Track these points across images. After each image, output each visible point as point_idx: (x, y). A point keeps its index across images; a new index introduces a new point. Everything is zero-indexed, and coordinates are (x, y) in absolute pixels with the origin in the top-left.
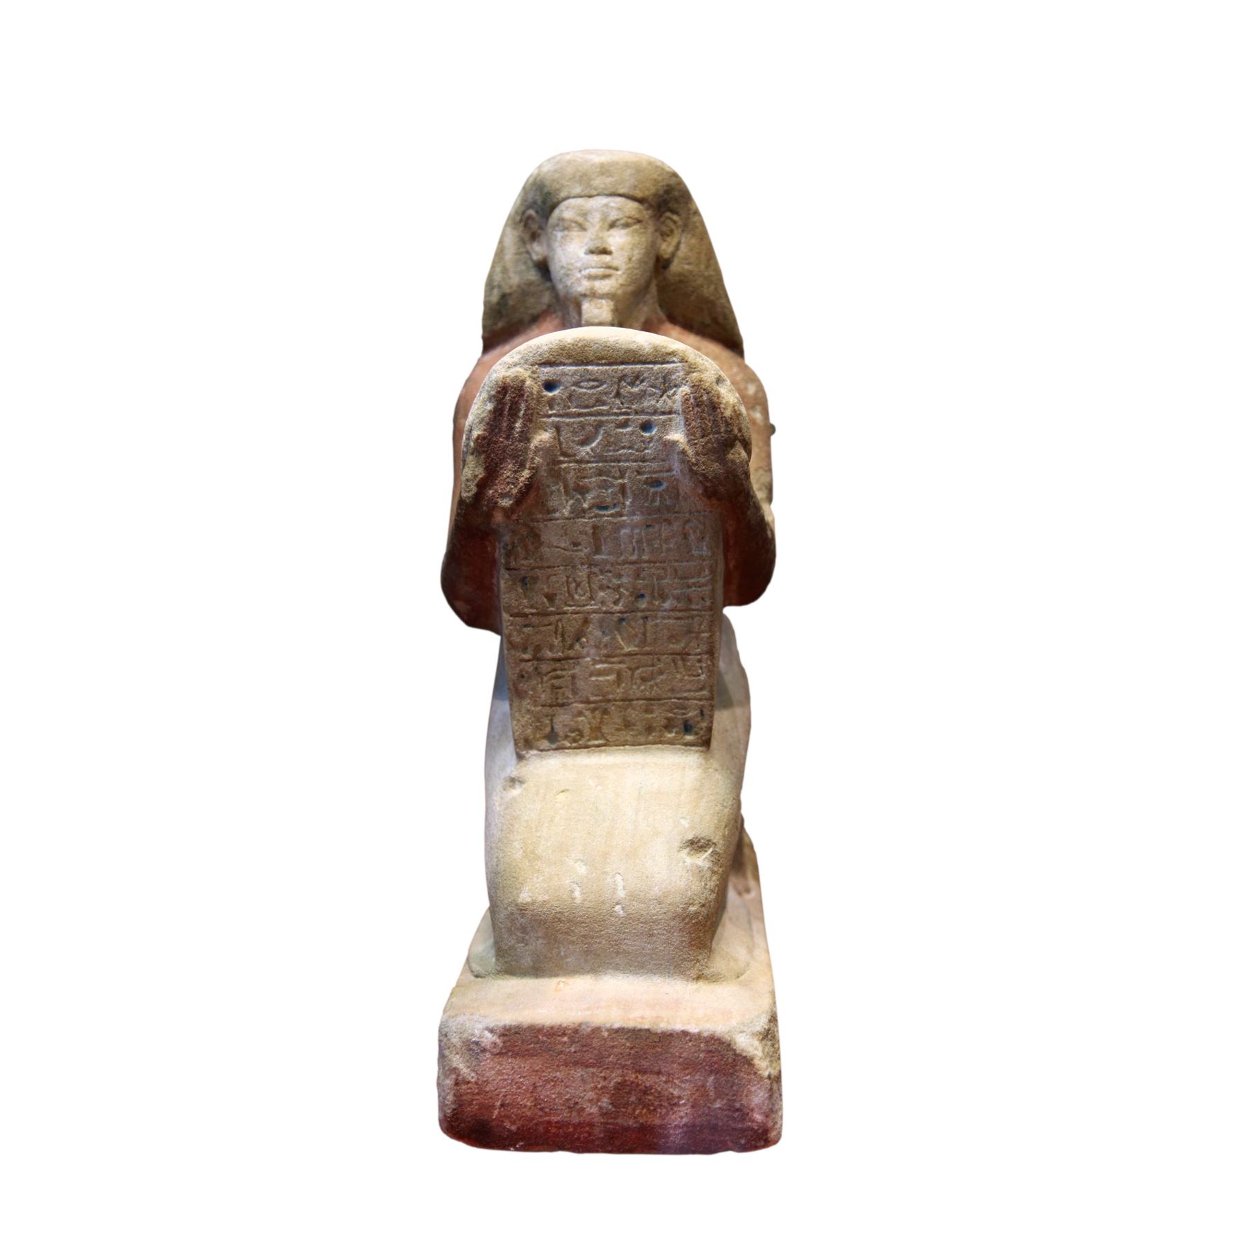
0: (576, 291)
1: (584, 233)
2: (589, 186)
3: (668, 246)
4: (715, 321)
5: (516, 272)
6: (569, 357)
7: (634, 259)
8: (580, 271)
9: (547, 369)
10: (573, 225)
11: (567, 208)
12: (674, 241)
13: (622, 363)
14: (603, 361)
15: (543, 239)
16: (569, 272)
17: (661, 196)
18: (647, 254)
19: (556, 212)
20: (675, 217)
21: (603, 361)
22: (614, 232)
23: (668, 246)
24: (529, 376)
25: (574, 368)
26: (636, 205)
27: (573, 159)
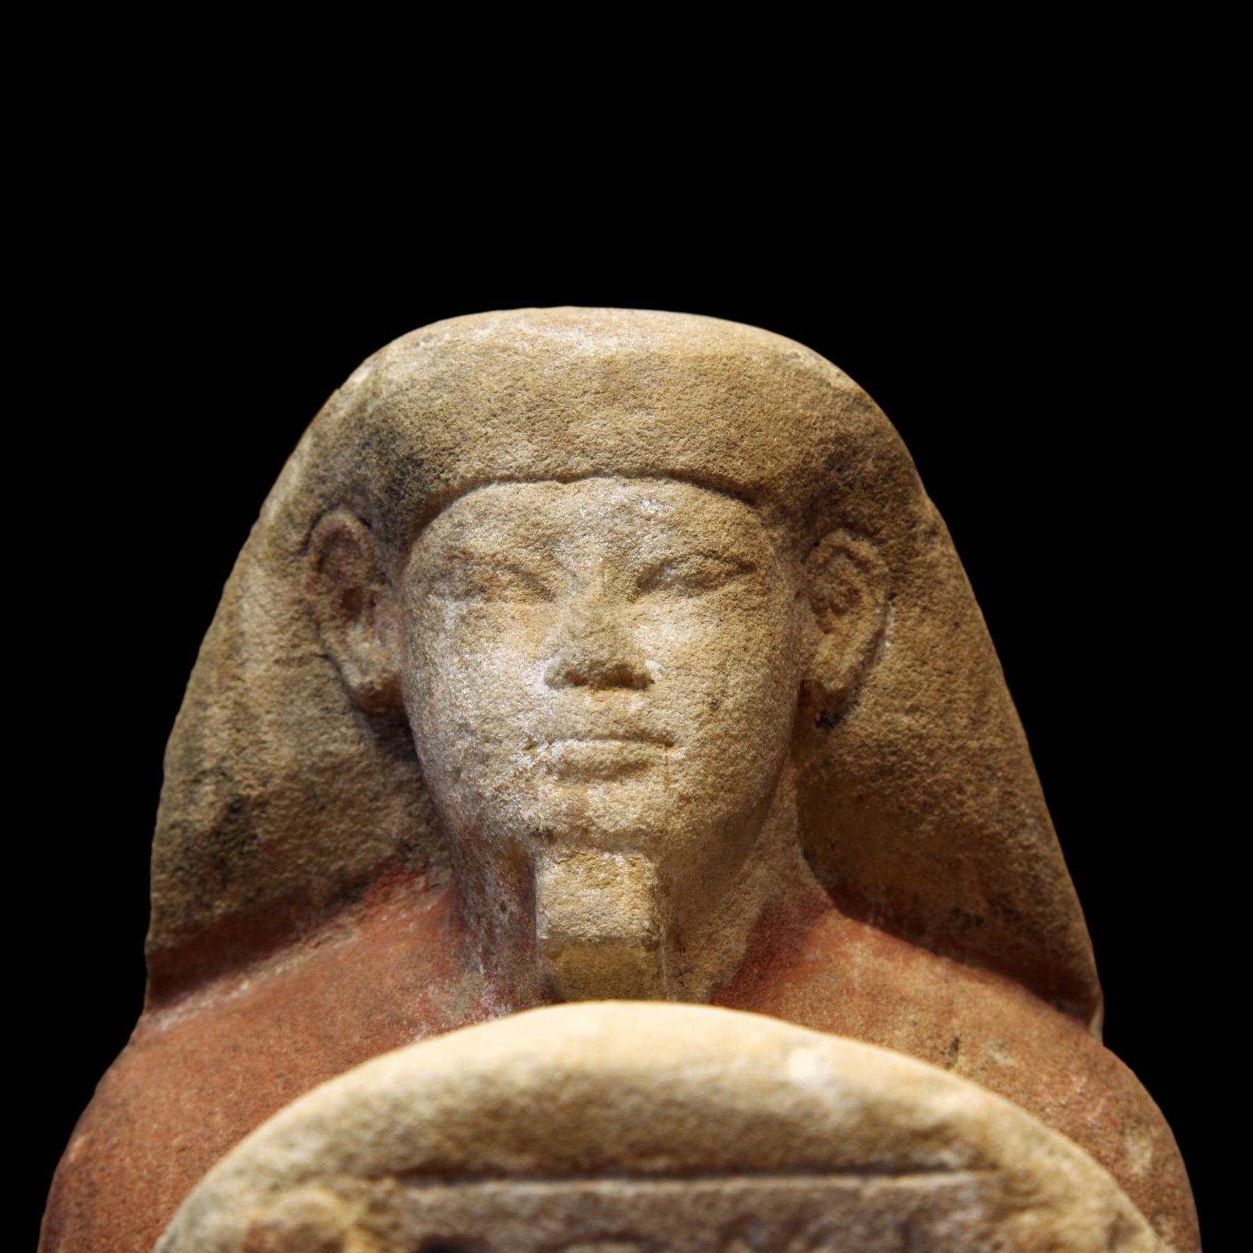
0: (515, 819)
1: (541, 606)
2: (562, 438)
3: (840, 648)
4: (1001, 904)
5: (279, 725)
6: (523, 1143)
7: (729, 703)
8: (531, 746)
9: (430, 1196)
10: (506, 577)
11: (481, 516)
12: (863, 631)
13: (734, 1169)
14: (661, 1163)
15: (386, 612)
16: (488, 748)
17: (817, 477)
18: (774, 680)
19: (442, 527)
20: (864, 549)
21: (661, 1163)
22: (650, 604)
23: (840, 648)
24: (361, 1226)
25: (538, 1190)
26: (732, 508)
27: (501, 342)
